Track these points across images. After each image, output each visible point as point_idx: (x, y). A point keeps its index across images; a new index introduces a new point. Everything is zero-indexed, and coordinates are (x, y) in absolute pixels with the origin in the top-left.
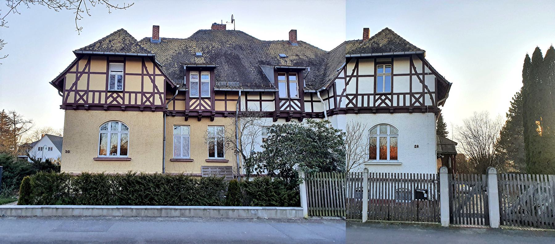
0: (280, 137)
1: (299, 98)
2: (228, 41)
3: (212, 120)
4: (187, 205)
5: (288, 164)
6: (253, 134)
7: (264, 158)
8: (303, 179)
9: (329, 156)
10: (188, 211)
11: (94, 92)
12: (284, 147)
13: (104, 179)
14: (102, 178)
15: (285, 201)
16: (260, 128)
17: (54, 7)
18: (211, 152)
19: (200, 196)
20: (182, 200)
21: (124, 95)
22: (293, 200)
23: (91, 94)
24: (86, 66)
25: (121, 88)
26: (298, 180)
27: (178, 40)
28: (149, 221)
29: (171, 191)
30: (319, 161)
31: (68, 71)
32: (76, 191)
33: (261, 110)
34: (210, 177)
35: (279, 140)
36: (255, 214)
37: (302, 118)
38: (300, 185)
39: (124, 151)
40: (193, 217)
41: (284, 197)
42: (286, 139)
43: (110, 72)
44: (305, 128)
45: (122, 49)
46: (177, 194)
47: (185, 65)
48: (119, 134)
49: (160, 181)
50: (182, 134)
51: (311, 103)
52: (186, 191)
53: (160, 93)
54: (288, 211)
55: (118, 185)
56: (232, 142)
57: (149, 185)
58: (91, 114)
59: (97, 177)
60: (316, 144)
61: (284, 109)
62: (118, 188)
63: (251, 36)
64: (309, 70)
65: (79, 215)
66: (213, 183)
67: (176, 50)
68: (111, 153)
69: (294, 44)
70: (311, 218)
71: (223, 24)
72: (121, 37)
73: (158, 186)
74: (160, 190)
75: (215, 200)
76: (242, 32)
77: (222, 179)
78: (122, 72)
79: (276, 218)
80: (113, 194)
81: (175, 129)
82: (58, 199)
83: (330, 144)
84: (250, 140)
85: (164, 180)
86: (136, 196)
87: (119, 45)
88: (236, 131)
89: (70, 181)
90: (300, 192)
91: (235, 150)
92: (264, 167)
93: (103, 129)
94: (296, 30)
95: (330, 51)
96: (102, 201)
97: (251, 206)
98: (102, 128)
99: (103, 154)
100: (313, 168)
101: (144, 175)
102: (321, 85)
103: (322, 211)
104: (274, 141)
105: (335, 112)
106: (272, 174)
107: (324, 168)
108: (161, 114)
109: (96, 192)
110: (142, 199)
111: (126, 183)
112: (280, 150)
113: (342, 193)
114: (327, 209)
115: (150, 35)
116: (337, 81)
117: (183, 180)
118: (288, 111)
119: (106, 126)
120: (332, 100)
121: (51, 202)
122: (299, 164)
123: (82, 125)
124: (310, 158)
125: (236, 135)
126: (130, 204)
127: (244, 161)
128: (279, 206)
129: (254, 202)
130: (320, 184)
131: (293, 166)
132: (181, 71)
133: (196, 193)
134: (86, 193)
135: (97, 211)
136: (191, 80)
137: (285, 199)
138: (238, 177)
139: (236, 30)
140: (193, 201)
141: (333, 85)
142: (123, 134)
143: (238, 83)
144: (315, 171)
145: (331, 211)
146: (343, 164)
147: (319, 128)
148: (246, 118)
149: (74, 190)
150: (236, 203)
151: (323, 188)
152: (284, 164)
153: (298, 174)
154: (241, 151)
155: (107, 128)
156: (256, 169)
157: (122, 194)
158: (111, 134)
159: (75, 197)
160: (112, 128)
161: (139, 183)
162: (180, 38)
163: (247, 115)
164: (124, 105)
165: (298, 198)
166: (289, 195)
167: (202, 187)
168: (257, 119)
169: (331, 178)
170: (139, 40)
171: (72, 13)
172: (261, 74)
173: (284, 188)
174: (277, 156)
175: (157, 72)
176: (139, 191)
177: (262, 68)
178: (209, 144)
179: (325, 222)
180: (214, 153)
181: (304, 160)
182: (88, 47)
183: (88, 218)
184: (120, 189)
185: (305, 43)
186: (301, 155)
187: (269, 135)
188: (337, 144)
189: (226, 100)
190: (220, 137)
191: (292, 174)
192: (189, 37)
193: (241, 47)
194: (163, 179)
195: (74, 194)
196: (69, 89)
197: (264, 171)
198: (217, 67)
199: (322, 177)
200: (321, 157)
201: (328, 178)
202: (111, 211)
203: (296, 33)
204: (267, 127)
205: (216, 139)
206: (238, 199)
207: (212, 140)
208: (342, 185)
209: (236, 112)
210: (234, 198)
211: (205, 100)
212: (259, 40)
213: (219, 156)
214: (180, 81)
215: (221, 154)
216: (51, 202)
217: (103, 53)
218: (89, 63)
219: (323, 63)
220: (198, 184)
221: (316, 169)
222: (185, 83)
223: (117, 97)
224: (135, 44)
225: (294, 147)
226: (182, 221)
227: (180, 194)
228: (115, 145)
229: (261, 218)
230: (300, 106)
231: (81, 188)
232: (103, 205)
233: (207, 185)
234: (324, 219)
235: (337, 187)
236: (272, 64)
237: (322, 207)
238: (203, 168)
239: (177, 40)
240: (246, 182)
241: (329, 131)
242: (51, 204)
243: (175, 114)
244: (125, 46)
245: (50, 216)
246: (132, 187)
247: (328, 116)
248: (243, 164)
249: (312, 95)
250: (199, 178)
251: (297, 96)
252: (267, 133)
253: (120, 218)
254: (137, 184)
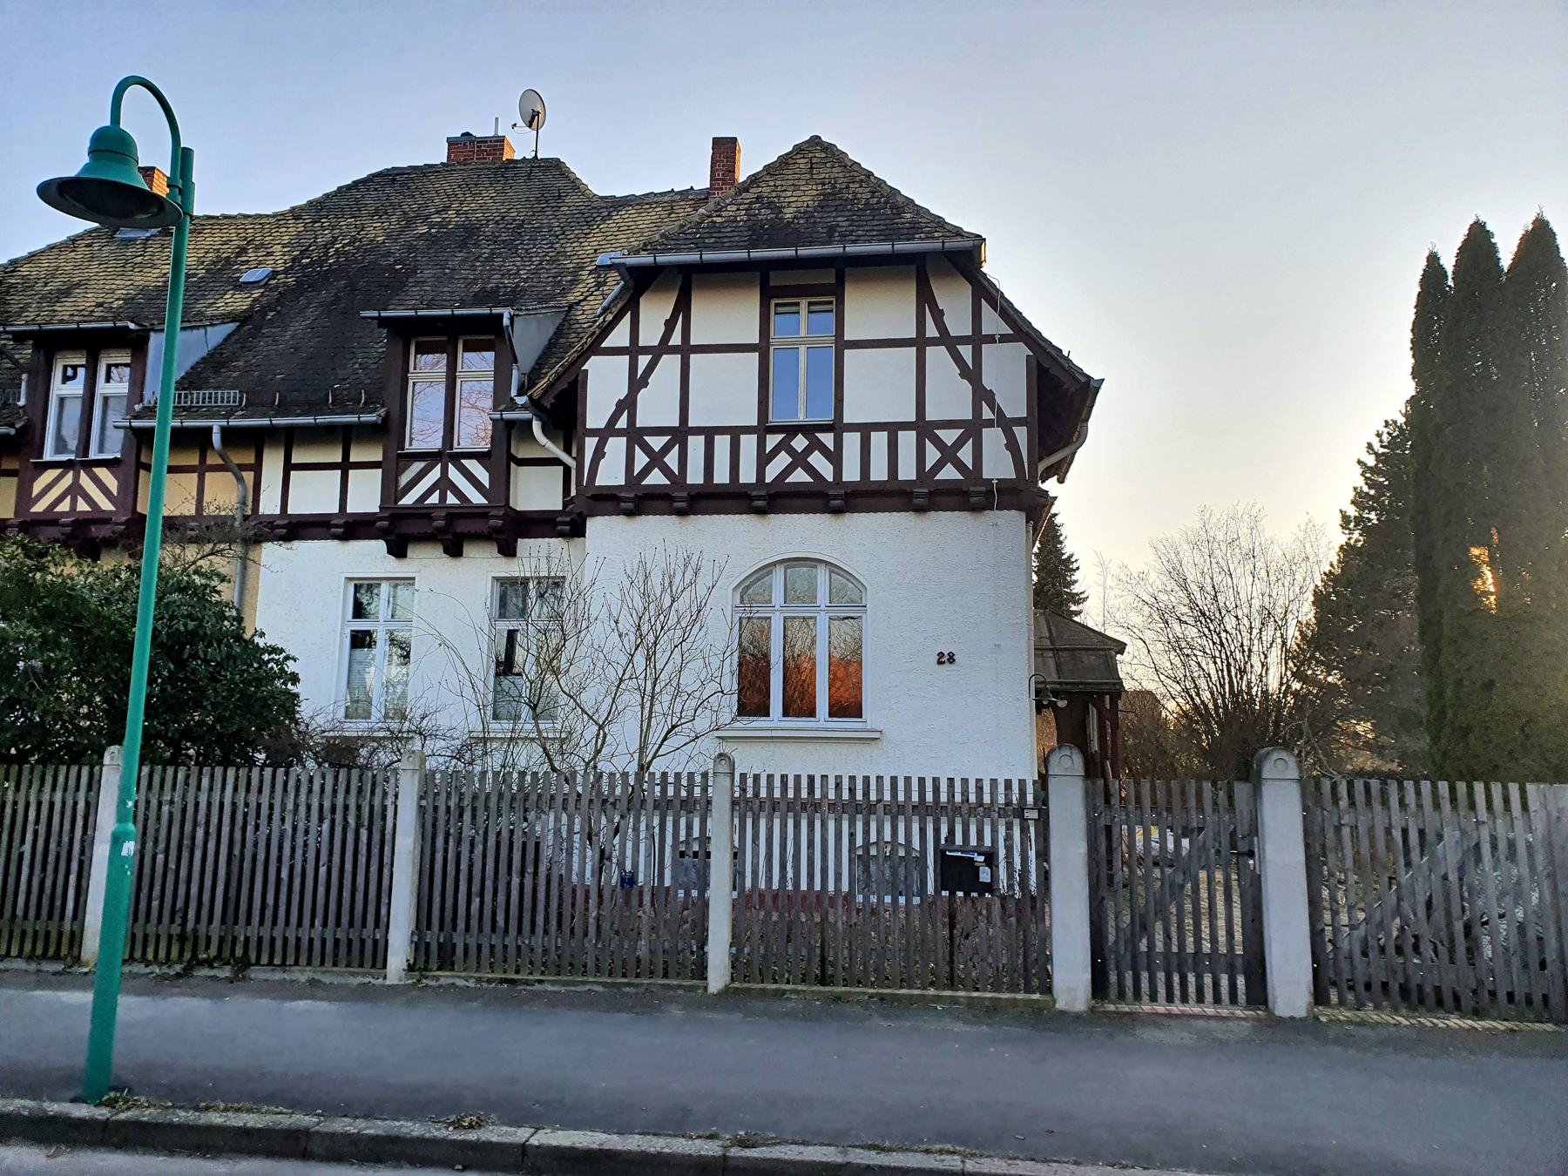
21: (839, 443)
23: (696, 444)
53: (1006, 424)
223: (808, 451)
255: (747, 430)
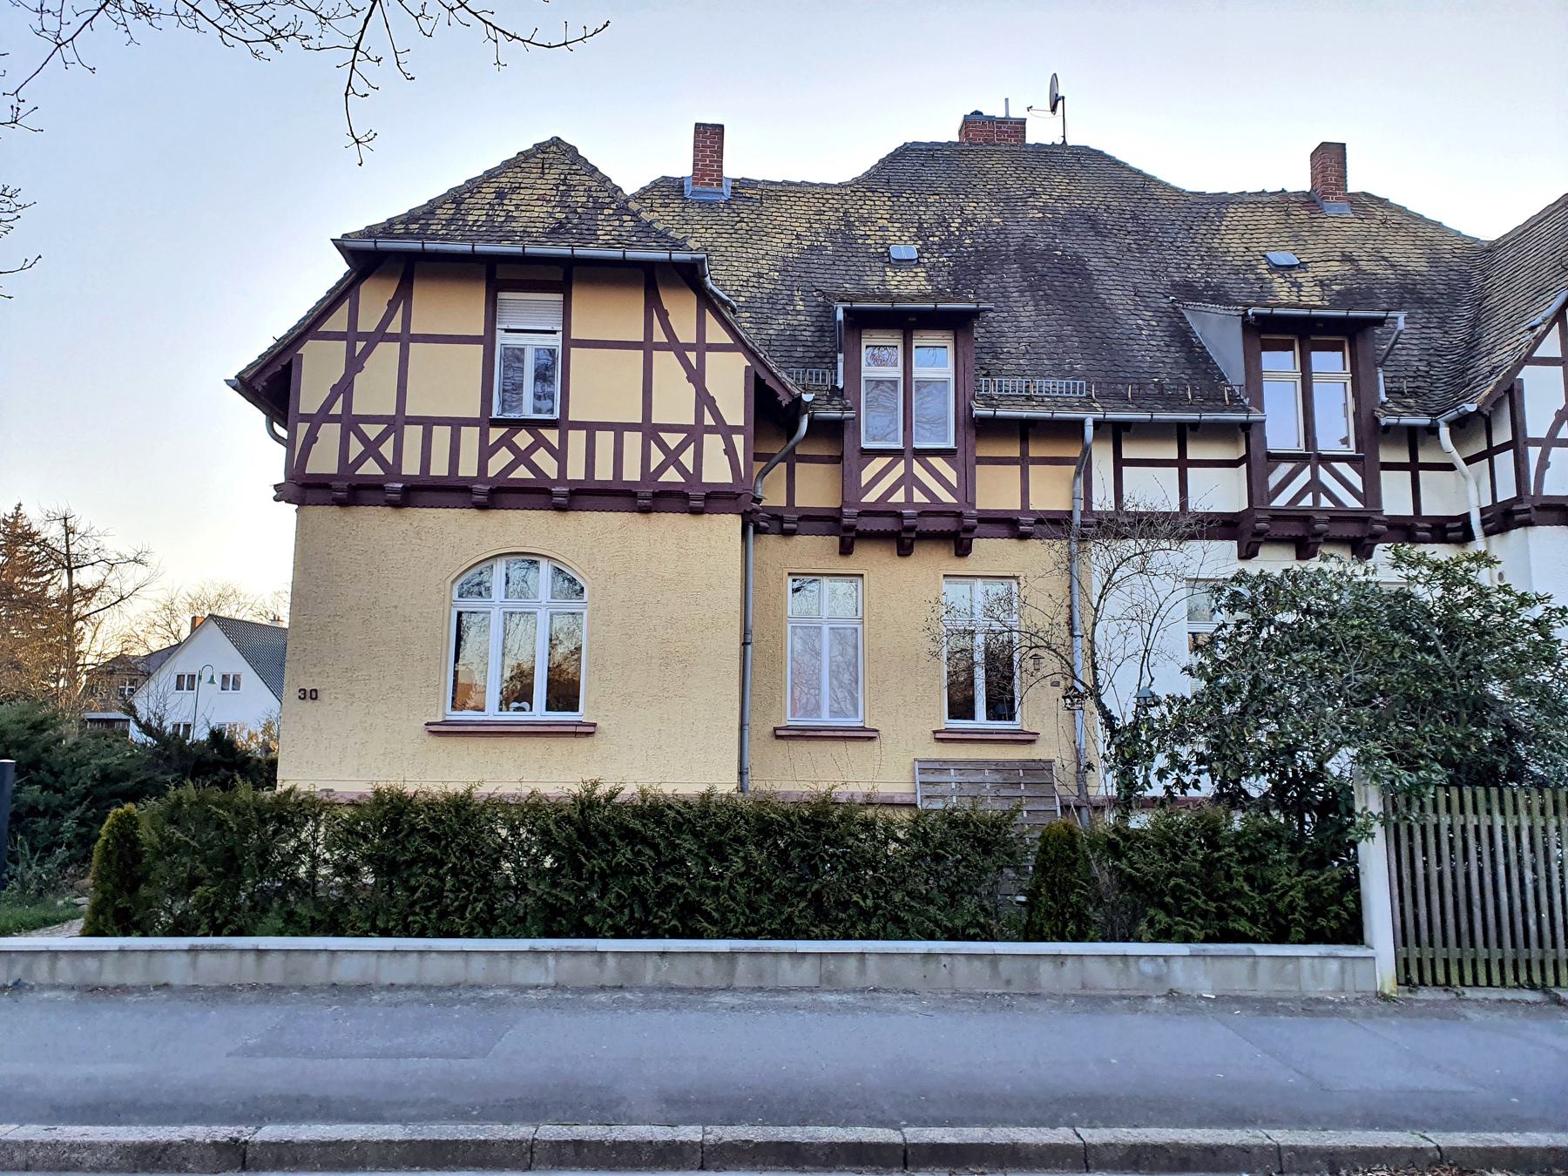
0: (1268, 626)
1: (1358, 451)
2: (1034, 194)
3: (963, 550)
4: (847, 936)
5: (1307, 749)
6: (1148, 617)
7: (1198, 724)
8: (1377, 818)
9: (1492, 714)
10: (852, 963)
11: (428, 423)
12: (1290, 673)
13: (475, 816)
14: (463, 812)
15: (1294, 920)
16: (1178, 586)
17: (246, 42)
18: (958, 697)
19: (909, 894)
20: (827, 914)
21: (563, 440)
22: (1329, 911)
23: (413, 434)
24: (392, 306)
25: (550, 405)
26: (1352, 823)
27: (810, 189)
28: (677, 1008)
29: (775, 873)
30: (1444, 736)
31: (310, 328)
32: (349, 874)
33: (1184, 505)
34: (954, 809)
35: (1266, 641)
36: (1159, 979)
37: (1368, 541)
38: (1362, 846)
39: (564, 693)
40: (875, 990)
41: (1287, 899)
42: (1298, 637)
43: (500, 334)
44: (1384, 587)
45: (554, 228)
46: (806, 887)
47: (842, 301)
48: (543, 617)
49: (728, 826)
50: (825, 614)
51: (1408, 474)
52: (845, 872)
53: (726, 431)
54: (1306, 963)
55: (535, 843)
56: (1054, 651)
57: (675, 847)
58: (415, 524)
59: (443, 811)
60: (1431, 659)
61: (1289, 503)
62: (536, 860)
63: (1139, 172)
64: (1401, 325)
65: (362, 981)
66: (967, 838)
67: (798, 237)
68: (505, 703)
69: (1333, 207)
70: (1408, 995)
71: (1012, 115)
72: (552, 176)
73: (717, 851)
74: (727, 869)
75: (975, 915)
76: (1100, 154)
77: (1009, 819)
78: (554, 332)
79: (1250, 994)
80: (515, 888)
81: (796, 590)
82: (265, 911)
83: (1495, 660)
84: (1136, 643)
85: (747, 822)
86: (619, 896)
87: (540, 211)
88: (1072, 601)
89: (318, 826)
90: (1361, 876)
91: (1068, 689)
92: (1199, 762)
93: (470, 592)
94: (1344, 145)
95: (1499, 240)
96: (462, 917)
97: (1139, 940)
98: (465, 587)
99: (471, 703)
100: (1420, 768)
101: (656, 798)
102: (1455, 393)
103: (1460, 963)
104: (1245, 644)
105: (1518, 517)
106: (1232, 797)
107: (1470, 768)
108: (733, 523)
109: (436, 876)
110: (647, 911)
111: (575, 836)
112: (1270, 685)
113: (1549, 879)
114: (1483, 953)
115: (682, 166)
116: (1527, 374)
117: (831, 822)
118: (1307, 509)
119: (485, 577)
120: (1505, 461)
121: (233, 922)
122: (1356, 750)
123: (376, 573)
124: (1409, 724)
125: (1071, 618)
126: (592, 934)
127: (1108, 739)
128: (1266, 942)
129: (1151, 923)
130: (1451, 840)
131: (1329, 758)
132: (821, 330)
133: (888, 881)
134: (390, 883)
135: (443, 961)
136: (868, 371)
137: (1292, 907)
138: (1078, 808)
139: (1070, 143)
140: (875, 920)
141: (1512, 394)
142: (558, 614)
143: (1081, 385)
144: (1427, 783)
145: (1501, 963)
146: (1554, 751)
147: (1447, 588)
148: (1115, 544)
149: (336, 866)
150: (1071, 926)
151: (1466, 858)
152: (1290, 751)
153: (1352, 797)
154: (1095, 692)
155: (488, 589)
156: (1162, 774)
157: (555, 885)
158: (505, 613)
159: (342, 899)
160: (512, 587)
161: (629, 835)
162: (818, 182)
163: (1123, 530)
164: (564, 486)
165: (1353, 906)
166: (1313, 891)
167: (920, 856)
168: (1165, 544)
169: (1502, 812)
170: (630, 188)
171: (330, 67)
172: (1183, 344)
173: (1289, 860)
174: (1257, 712)
175: (716, 333)
176: (630, 873)
177: (1189, 318)
178: (949, 659)
179: (1474, 1015)
180: (971, 701)
181: (1379, 731)
182: (402, 223)
183: (401, 996)
184: (548, 862)
185: (1383, 202)
186: (1367, 709)
187: (1220, 617)
188: (1526, 662)
189: (1024, 462)
190: (997, 626)
191: (1325, 796)
192: (858, 173)
193: (1093, 223)
194: (743, 817)
195: (337, 887)
196: (728, 424)
197: (1197, 781)
198: (984, 310)
199: (1462, 811)
200: (1453, 718)
201: (1489, 812)
202: (504, 964)
203: (1345, 158)
204: (1212, 583)
205: (980, 639)
206: (1079, 909)
207: (961, 644)
208: (1553, 847)
209: (1070, 513)
210: (1063, 906)
211: (930, 460)
212: (1176, 190)
213: (994, 712)
214: (817, 374)
215: (1001, 706)
216: (233, 922)
217: (467, 247)
218: (404, 295)
219: (1467, 295)
220: (897, 840)
221: (1434, 771)
222: (840, 385)
223: (532, 449)
224: (614, 206)
225: (1332, 671)
226: (826, 1008)
227: (816, 887)
228: (526, 667)
229: (1186, 993)
230: (1360, 488)
231: (368, 859)
232: (470, 935)
233: (942, 845)
234: (1468, 1000)
235: (1527, 856)
236: (1234, 295)
237: (1459, 944)
238: (923, 771)
239: (803, 188)
240: (1116, 830)
241: (1494, 600)
242: (233, 934)
243: (795, 526)
244: (570, 216)
245: (231, 988)
246: (602, 853)
247: (1488, 533)
248: (1102, 748)
249: (1413, 438)
250: (905, 815)
251: (1345, 441)
252: (1213, 610)
253: (544, 994)
254: (622, 838)
255: (632, 427)
